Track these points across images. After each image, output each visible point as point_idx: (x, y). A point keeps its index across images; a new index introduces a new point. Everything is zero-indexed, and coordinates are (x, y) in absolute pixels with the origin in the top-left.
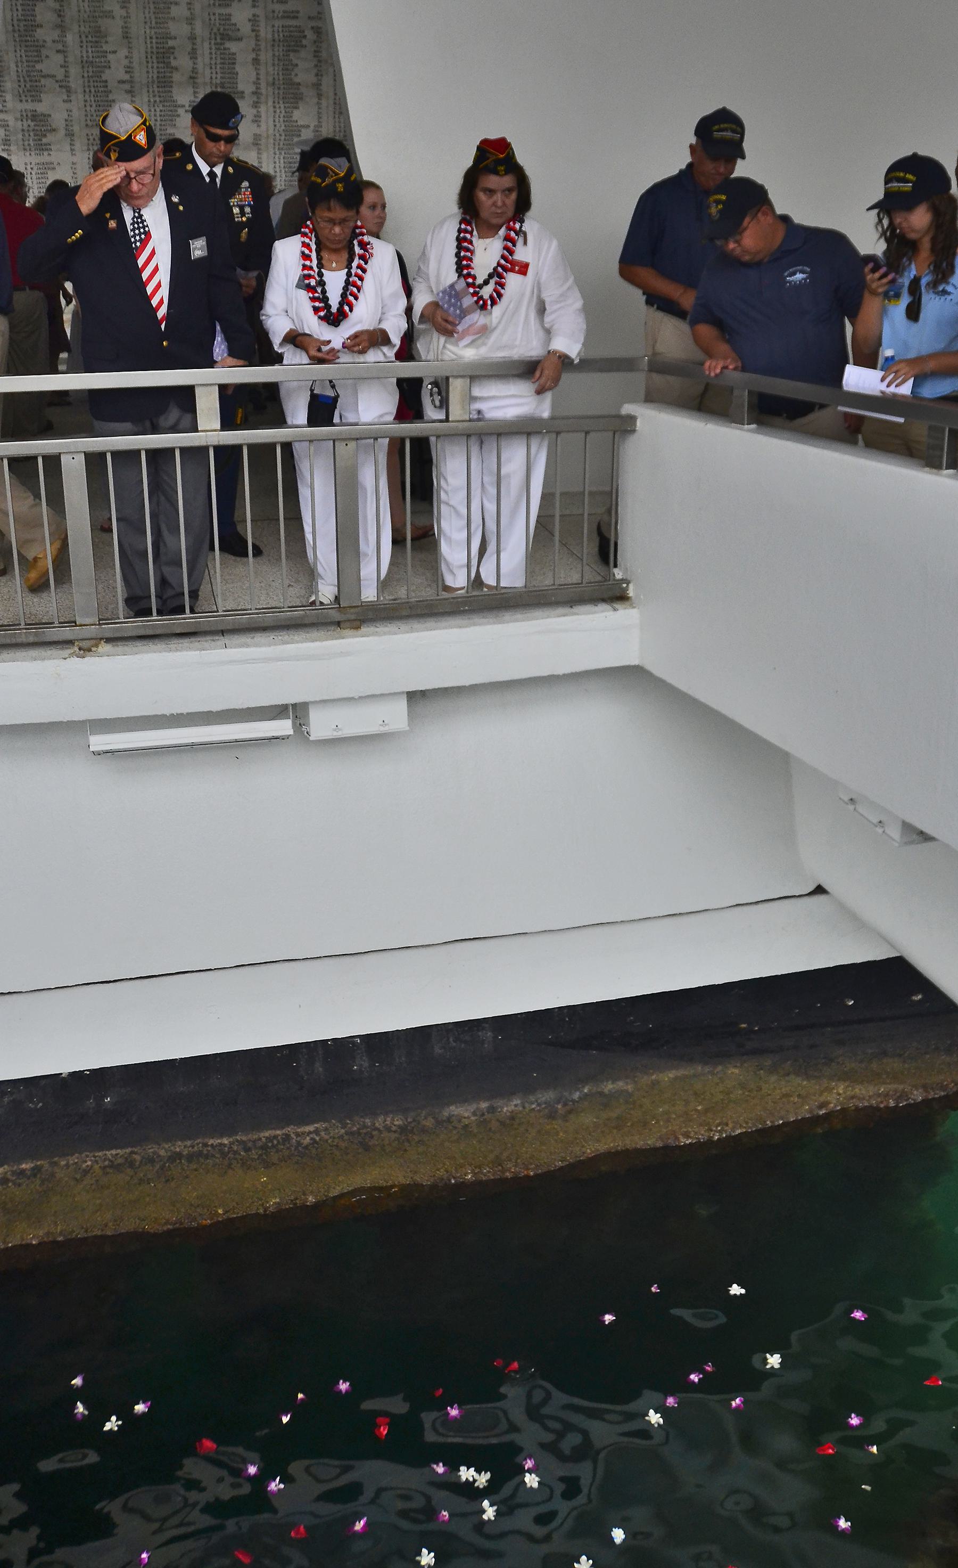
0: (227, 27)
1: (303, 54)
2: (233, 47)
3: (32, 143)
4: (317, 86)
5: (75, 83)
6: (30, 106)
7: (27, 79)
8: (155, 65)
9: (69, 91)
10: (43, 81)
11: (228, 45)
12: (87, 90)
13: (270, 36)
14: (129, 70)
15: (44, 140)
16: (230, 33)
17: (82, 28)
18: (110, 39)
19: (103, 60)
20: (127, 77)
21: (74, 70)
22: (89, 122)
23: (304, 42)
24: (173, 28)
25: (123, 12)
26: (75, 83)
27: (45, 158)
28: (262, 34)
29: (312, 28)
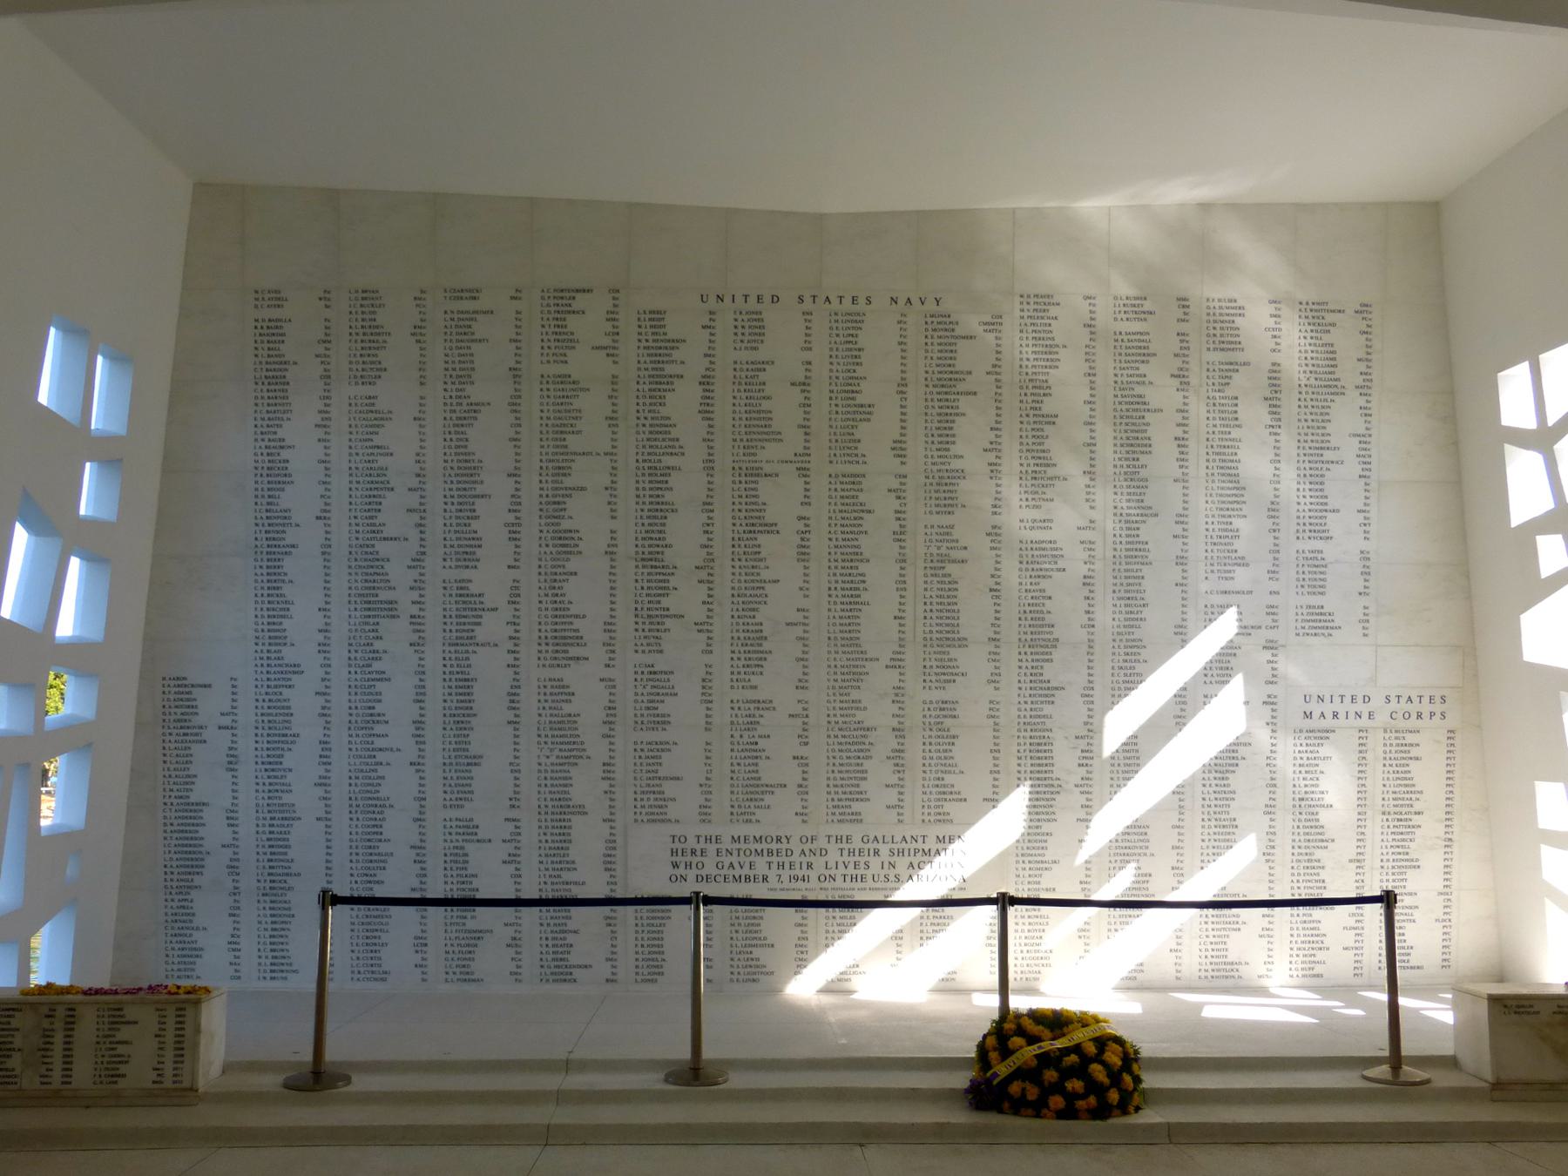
6: (648, 659)
10: (669, 623)
11: (950, 568)
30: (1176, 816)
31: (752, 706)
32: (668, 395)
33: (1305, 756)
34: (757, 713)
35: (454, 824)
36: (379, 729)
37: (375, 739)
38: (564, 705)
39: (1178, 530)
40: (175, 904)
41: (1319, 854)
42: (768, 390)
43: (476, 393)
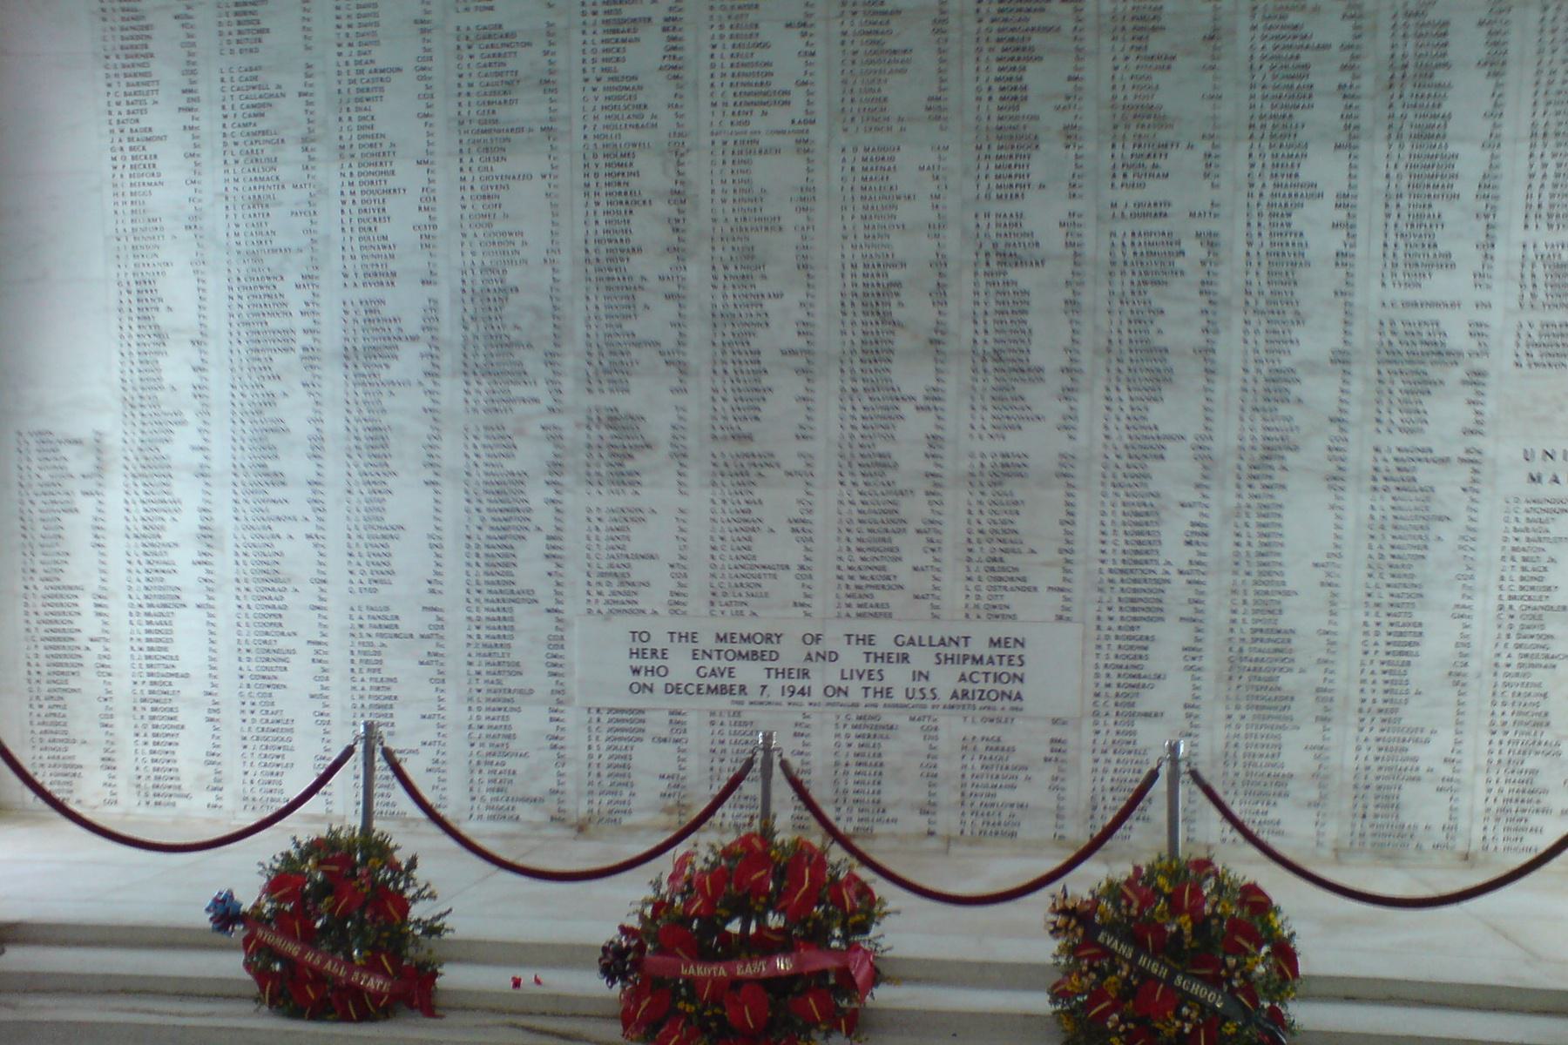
0: (1012, 240)
1: (1177, 286)
2: (1023, 277)
3: (604, 470)
4: (1206, 352)
5: (698, 356)
6: (606, 400)
7: (605, 350)
8: (860, 318)
9: (683, 369)
10: (633, 350)
11: (1013, 273)
12: (719, 368)
13: (1104, 256)
14: (805, 329)
15: (629, 465)
16: (1019, 251)
17: (719, 252)
18: (770, 270)
19: (754, 310)
20: (800, 343)
21: (698, 332)
22: (719, 433)
23: (1179, 263)
24: (899, 245)
25: (801, 219)
26: (698, 356)
27: (625, 499)
28: (1088, 250)
29: (1198, 235)
30: (1327, 617)
31: (745, 461)
32: (628, 46)
33: (1522, 536)
34: (753, 471)
35: (365, 613)
36: (275, 492)
37: (272, 506)
38: (504, 461)
39: (1341, 215)
40: (43, 712)
41: (1537, 675)
42: (765, 33)
43: (382, 56)
